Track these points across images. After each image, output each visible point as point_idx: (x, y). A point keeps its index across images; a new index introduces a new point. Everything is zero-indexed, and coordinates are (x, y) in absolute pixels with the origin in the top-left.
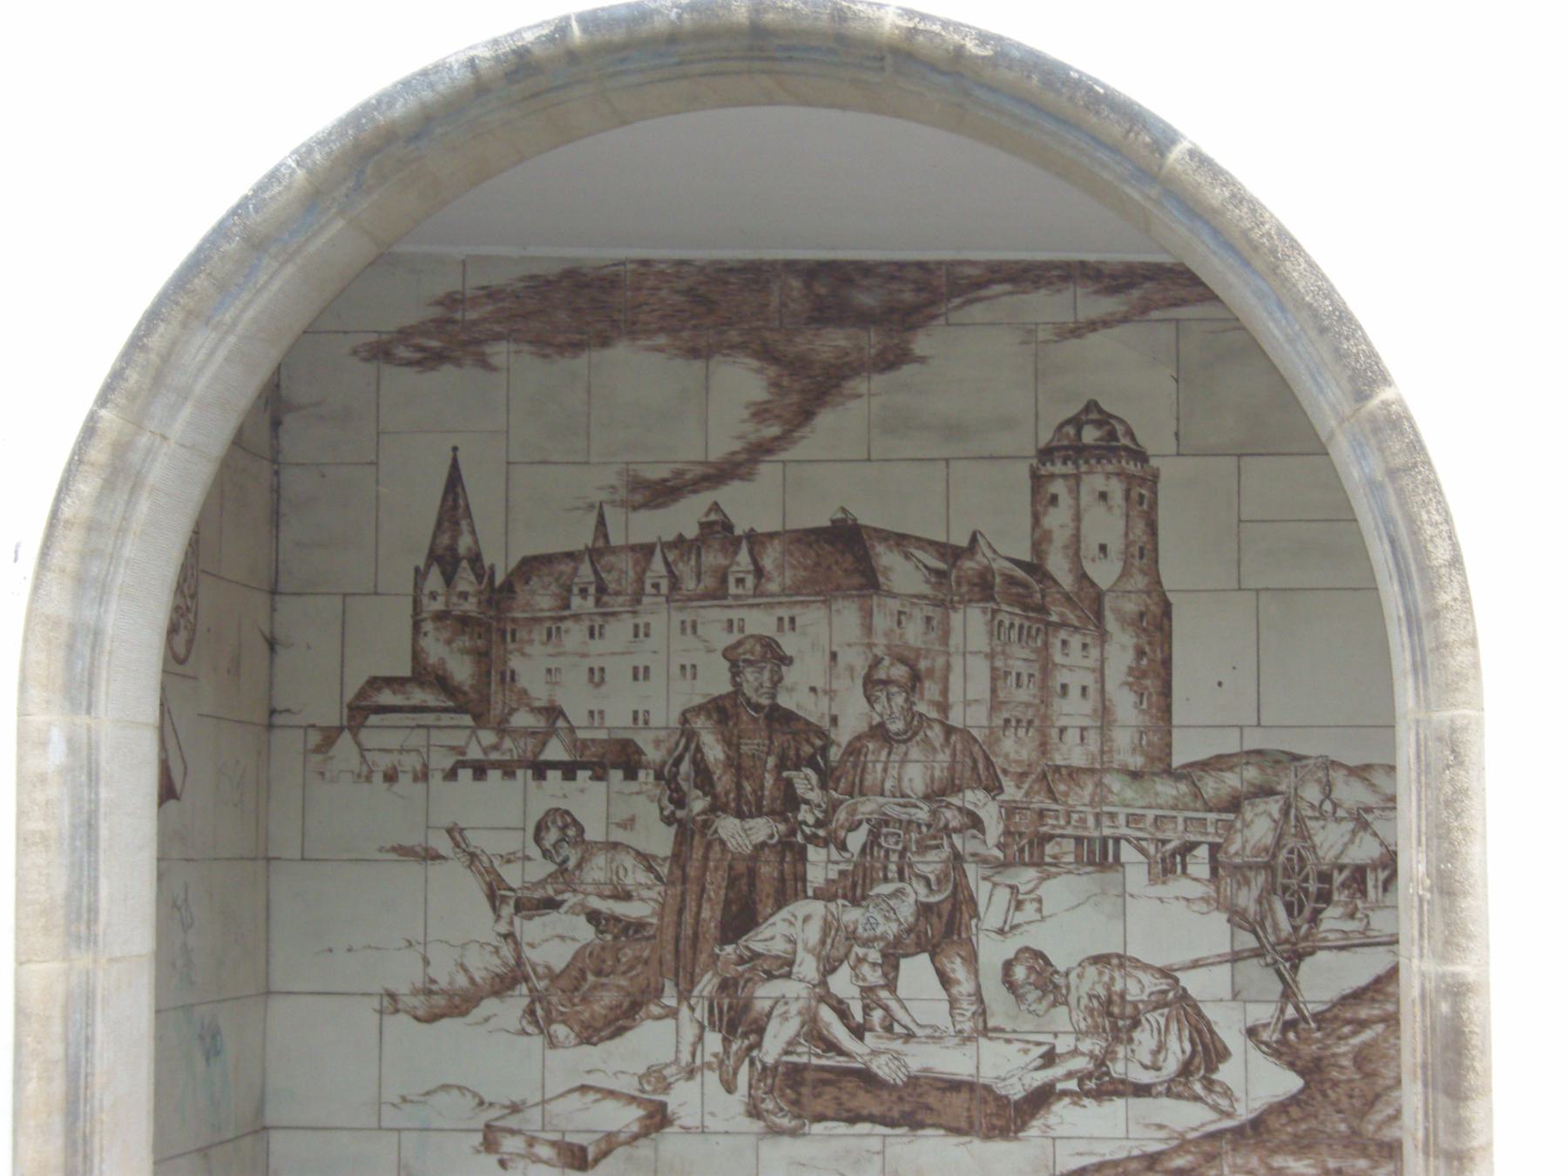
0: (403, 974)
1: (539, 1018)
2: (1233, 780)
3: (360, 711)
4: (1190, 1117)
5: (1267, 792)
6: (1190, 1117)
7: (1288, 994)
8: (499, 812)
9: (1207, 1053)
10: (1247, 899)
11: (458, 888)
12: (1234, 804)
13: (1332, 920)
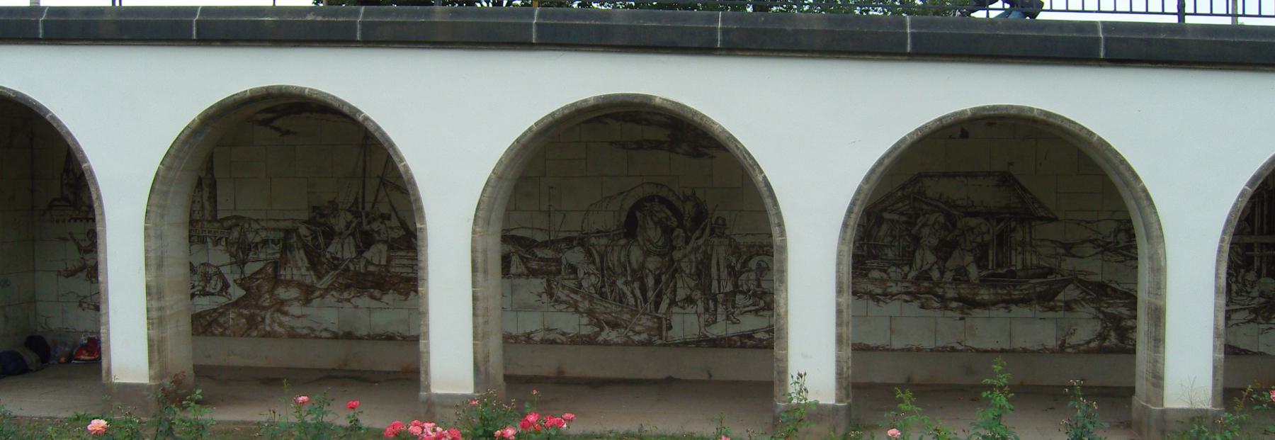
2: (230, 223)
3: (51, 206)
4: (223, 300)
5: (237, 225)
6: (223, 300)
7: (242, 272)
9: (226, 286)
10: (233, 250)
12: (230, 228)
13: (251, 255)
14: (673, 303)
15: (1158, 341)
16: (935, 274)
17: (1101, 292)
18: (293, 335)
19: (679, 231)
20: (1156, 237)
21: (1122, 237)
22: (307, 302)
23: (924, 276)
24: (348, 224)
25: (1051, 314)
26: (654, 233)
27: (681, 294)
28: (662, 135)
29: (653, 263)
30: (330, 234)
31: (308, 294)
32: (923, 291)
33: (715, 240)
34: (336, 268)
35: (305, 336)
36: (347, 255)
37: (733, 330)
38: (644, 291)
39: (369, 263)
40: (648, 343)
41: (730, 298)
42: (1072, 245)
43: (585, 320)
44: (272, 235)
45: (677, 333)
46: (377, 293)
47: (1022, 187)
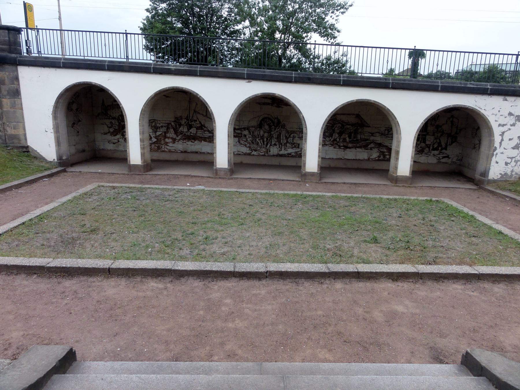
0: (103, 132)
1: (111, 135)
8: (108, 122)
11: (106, 127)
14: (271, 145)
15: (397, 159)
16: (338, 140)
17: (380, 145)
18: (170, 151)
19: (273, 127)
20: (399, 132)
21: (386, 132)
22: (174, 143)
23: (335, 140)
24: (185, 122)
25: (367, 151)
26: (267, 127)
27: (273, 143)
28: (269, 101)
29: (266, 135)
30: (180, 125)
31: (174, 140)
32: (334, 144)
33: (282, 129)
34: (182, 134)
35: (174, 152)
36: (185, 131)
37: (286, 152)
38: (263, 142)
39: (191, 133)
40: (264, 155)
41: (285, 144)
42: (373, 133)
43: (248, 149)
44: (164, 125)
45: (271, 153)
46: (193, 141)
47: (362, 119)
